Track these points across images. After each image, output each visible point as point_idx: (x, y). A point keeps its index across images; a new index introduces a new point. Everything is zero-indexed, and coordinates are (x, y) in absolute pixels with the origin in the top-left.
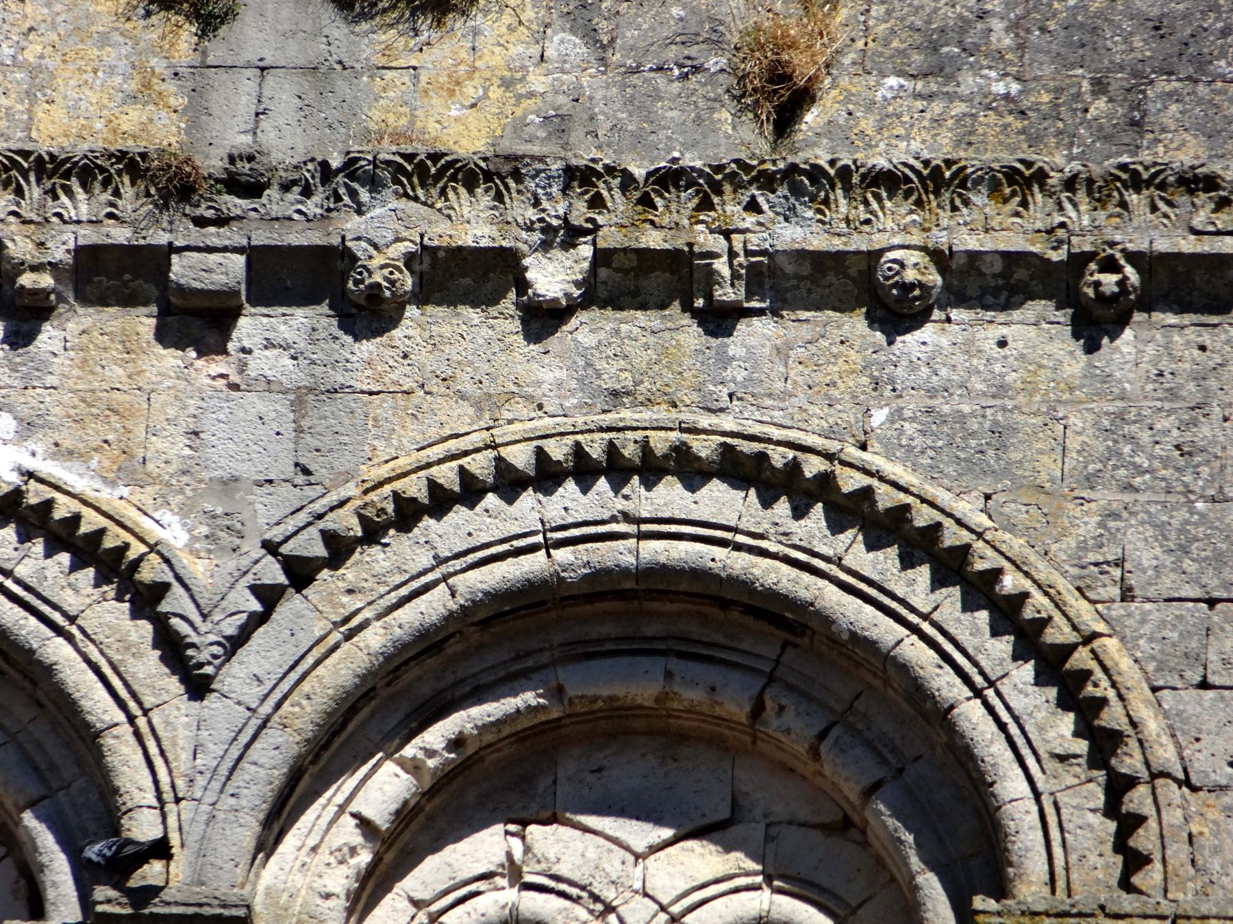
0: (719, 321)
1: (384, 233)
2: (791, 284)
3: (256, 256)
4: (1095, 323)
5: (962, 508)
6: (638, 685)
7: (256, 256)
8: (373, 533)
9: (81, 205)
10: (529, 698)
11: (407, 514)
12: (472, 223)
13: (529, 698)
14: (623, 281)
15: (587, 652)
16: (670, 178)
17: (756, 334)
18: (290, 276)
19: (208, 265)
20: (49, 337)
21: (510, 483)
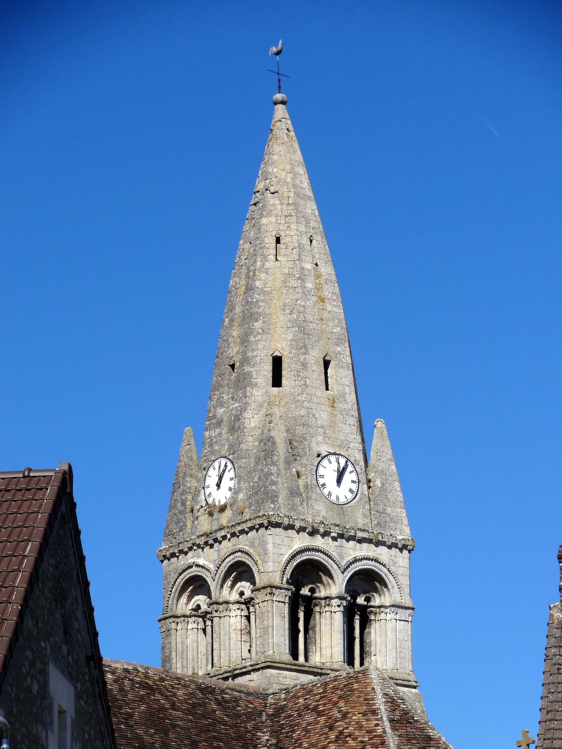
0: (238, 537)
1: (219, 535)
2: (242, 532)
3: (213, 540)
4: (257, 530)
5: (251, 551)
6: (241, 569)
7: (213, 540)
8: (222, 563)
9: (203, 538)
10: (235, 573)
11: (224, 560)
12: (223, 533)
13: (235, 573)
14: (233, 535)
15: (238, 567)
16: (232, 526)
17: (241, 537)
18: (216, 540)
19: (211, 542)
20: (205, 550)
21: (228, 556)
